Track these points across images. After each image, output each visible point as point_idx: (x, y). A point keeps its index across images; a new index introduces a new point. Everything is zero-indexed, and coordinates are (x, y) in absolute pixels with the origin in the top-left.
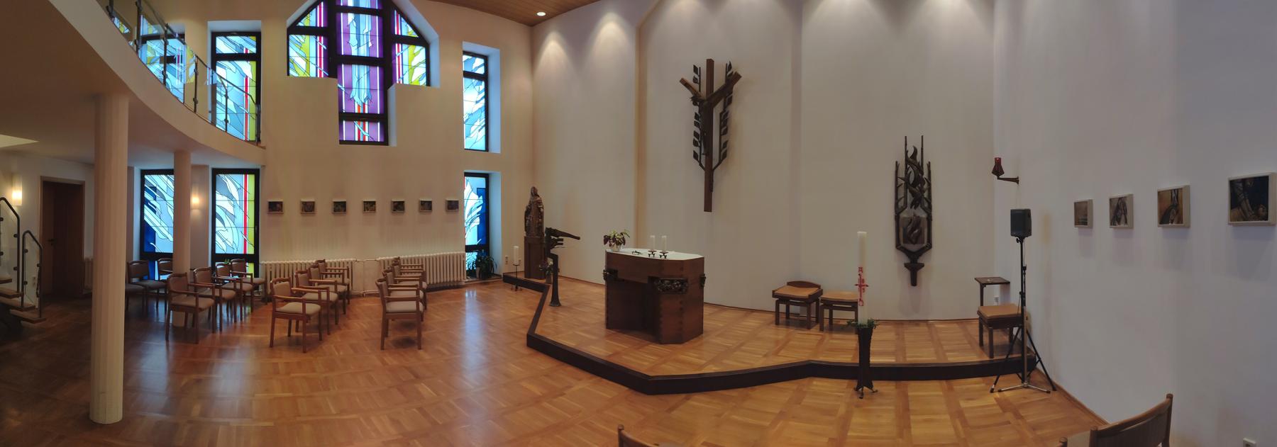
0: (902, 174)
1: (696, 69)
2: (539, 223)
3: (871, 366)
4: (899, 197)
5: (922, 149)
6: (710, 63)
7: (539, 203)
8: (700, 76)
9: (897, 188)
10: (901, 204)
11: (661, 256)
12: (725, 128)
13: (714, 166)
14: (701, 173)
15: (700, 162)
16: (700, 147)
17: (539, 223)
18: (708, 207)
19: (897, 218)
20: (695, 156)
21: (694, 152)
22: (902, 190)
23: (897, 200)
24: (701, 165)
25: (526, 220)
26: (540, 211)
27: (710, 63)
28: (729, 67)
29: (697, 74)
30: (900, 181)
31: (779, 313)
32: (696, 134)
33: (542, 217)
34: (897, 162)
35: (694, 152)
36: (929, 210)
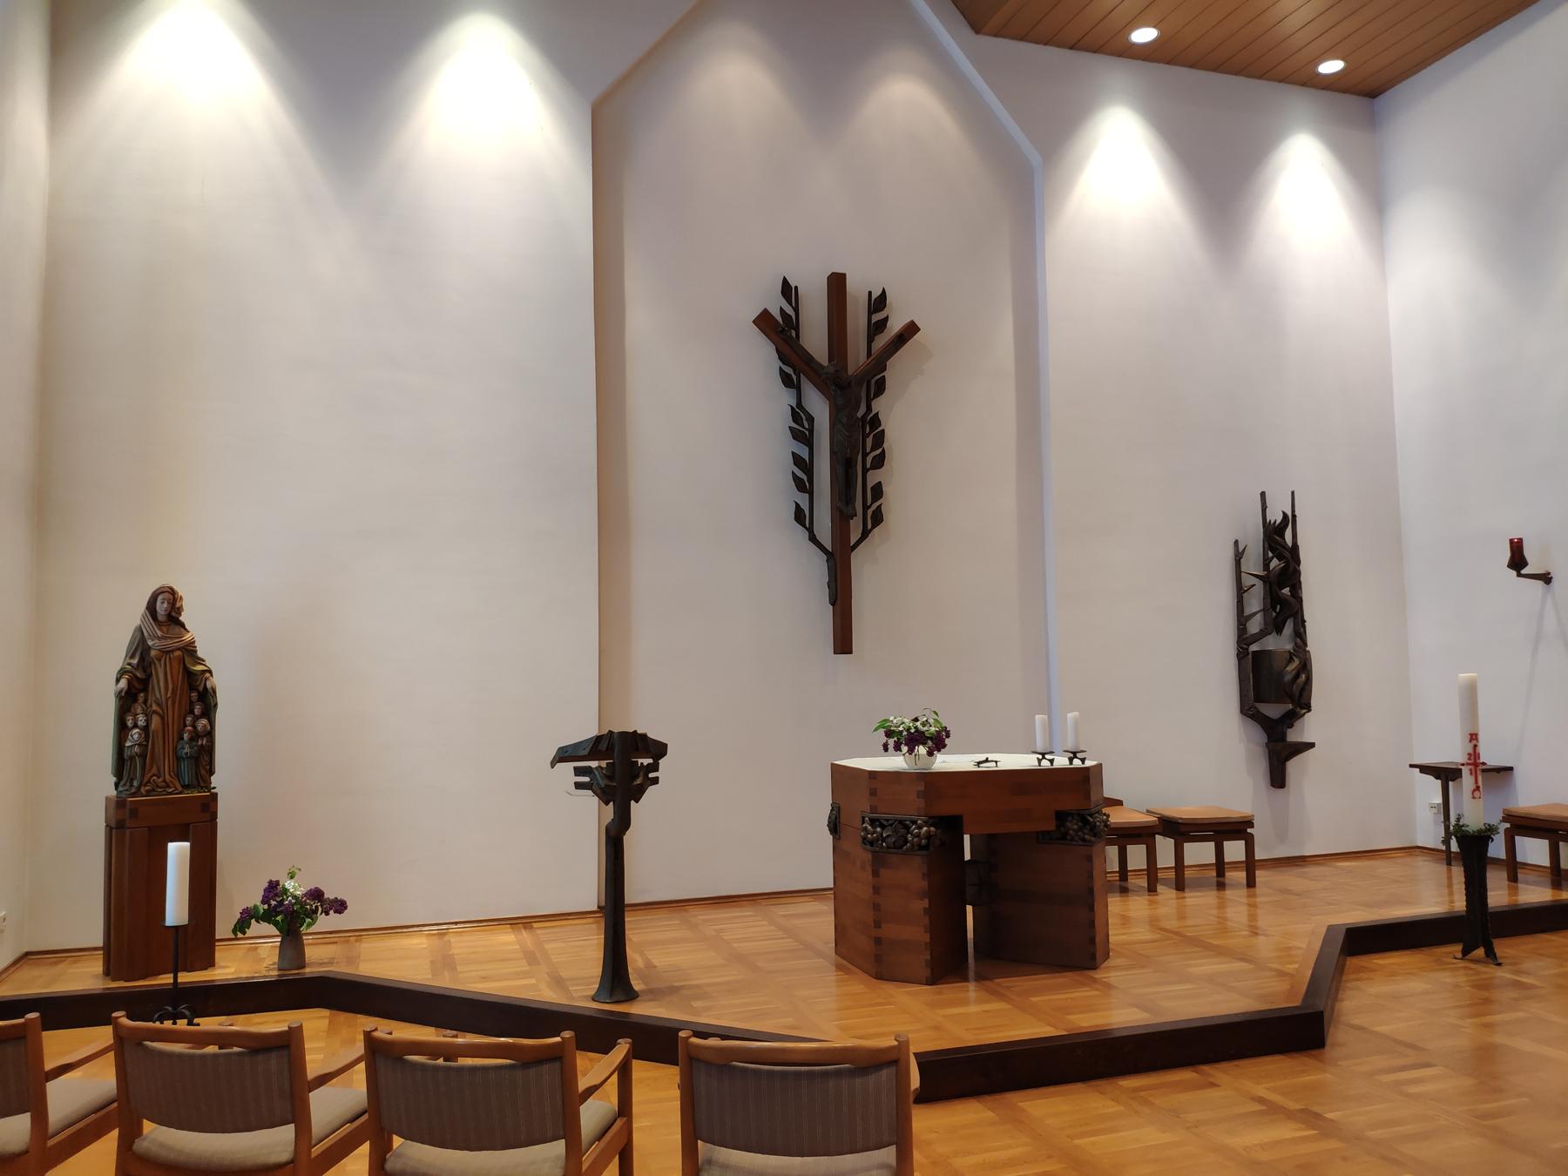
0: (1252, 564)
1: (787, 290)
2: (195, 736)
3: (1490, 911)
4: (1247, 612)
5: (1294, 516)
6: (837, 283)
7: (190, 650)
8: (796, 310)
9: (1241, 591)
10: (1254, 626)
11: (1039, 761)
12: (881, 450)
13: (853, 542)
14: (815, 567)
15: (810, 530)
16: (811, 493)
17: (195, 736)
18: (843, 644)
19: (1242, 654)
20: (799, 516)
21: (797, 505)
22: (1254, 603)
23: (1242, 620)
24: (813, 539)
25: (122, 729)
26: (192, 688)
27: (837, 283)
28: (878, 303)
29: (790, 304)
30: (1248, 581)
31: (1183, 866)
32: (797, 460)
33: (209, 710)
34: (1236, 542)
35: (797, 504)
36: (1300, 635)
